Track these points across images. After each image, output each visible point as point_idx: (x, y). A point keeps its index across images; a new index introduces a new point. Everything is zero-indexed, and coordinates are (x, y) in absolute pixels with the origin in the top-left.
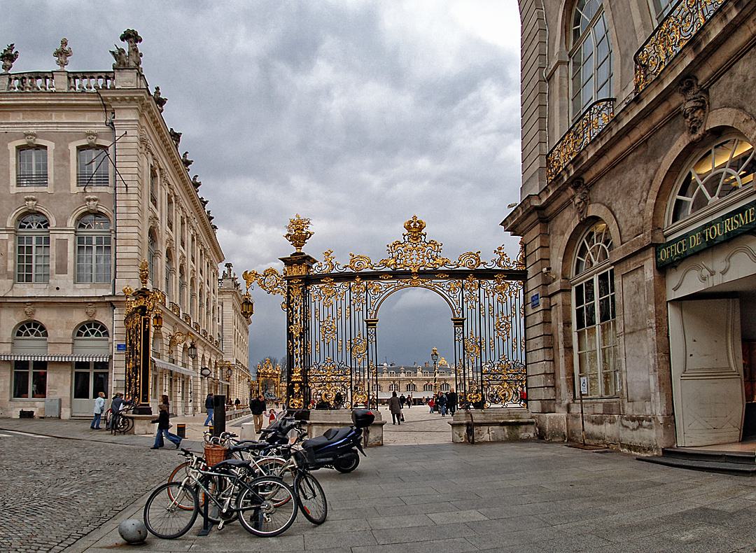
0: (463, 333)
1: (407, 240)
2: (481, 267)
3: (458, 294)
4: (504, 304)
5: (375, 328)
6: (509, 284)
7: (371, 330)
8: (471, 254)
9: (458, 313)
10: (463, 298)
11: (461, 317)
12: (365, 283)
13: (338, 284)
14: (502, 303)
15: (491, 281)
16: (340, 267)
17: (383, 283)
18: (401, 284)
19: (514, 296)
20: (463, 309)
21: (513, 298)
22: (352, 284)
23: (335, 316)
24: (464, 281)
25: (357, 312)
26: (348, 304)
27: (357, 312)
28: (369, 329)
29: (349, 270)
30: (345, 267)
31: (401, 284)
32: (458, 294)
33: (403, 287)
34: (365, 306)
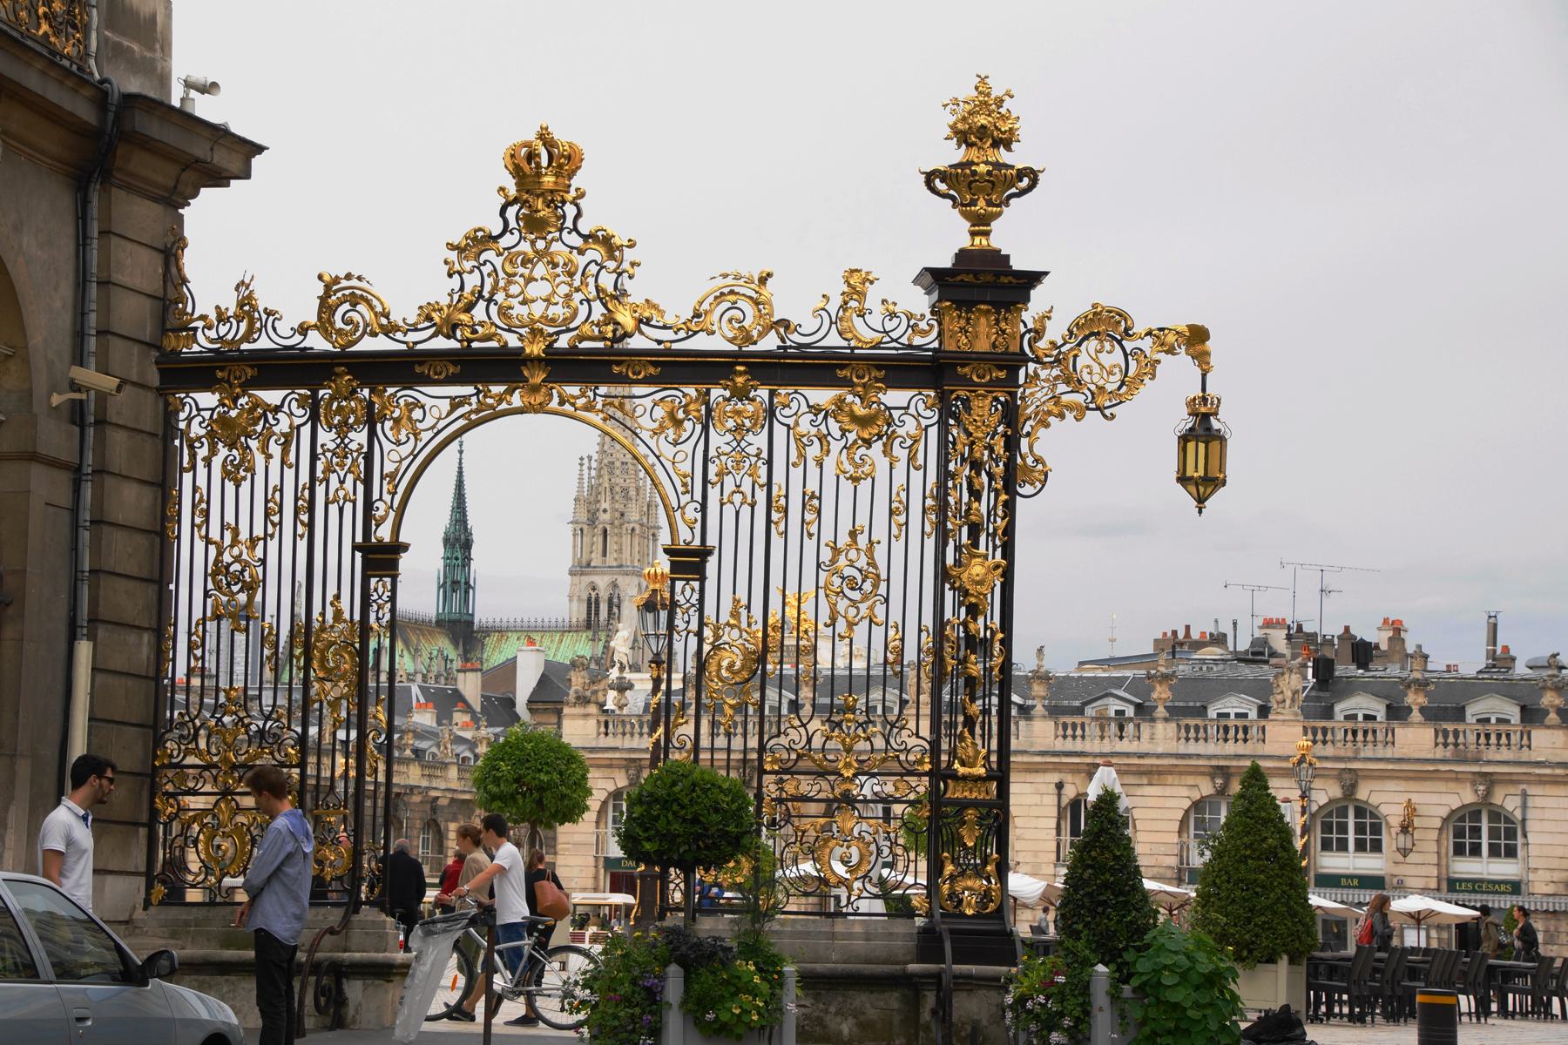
4: (865, 486)
7: (379, 586)
11: (697, 542)
14: (855, 480)
17: (435, 400)
21: (901, 467)
24: (717, 393)
30: (303, 330)
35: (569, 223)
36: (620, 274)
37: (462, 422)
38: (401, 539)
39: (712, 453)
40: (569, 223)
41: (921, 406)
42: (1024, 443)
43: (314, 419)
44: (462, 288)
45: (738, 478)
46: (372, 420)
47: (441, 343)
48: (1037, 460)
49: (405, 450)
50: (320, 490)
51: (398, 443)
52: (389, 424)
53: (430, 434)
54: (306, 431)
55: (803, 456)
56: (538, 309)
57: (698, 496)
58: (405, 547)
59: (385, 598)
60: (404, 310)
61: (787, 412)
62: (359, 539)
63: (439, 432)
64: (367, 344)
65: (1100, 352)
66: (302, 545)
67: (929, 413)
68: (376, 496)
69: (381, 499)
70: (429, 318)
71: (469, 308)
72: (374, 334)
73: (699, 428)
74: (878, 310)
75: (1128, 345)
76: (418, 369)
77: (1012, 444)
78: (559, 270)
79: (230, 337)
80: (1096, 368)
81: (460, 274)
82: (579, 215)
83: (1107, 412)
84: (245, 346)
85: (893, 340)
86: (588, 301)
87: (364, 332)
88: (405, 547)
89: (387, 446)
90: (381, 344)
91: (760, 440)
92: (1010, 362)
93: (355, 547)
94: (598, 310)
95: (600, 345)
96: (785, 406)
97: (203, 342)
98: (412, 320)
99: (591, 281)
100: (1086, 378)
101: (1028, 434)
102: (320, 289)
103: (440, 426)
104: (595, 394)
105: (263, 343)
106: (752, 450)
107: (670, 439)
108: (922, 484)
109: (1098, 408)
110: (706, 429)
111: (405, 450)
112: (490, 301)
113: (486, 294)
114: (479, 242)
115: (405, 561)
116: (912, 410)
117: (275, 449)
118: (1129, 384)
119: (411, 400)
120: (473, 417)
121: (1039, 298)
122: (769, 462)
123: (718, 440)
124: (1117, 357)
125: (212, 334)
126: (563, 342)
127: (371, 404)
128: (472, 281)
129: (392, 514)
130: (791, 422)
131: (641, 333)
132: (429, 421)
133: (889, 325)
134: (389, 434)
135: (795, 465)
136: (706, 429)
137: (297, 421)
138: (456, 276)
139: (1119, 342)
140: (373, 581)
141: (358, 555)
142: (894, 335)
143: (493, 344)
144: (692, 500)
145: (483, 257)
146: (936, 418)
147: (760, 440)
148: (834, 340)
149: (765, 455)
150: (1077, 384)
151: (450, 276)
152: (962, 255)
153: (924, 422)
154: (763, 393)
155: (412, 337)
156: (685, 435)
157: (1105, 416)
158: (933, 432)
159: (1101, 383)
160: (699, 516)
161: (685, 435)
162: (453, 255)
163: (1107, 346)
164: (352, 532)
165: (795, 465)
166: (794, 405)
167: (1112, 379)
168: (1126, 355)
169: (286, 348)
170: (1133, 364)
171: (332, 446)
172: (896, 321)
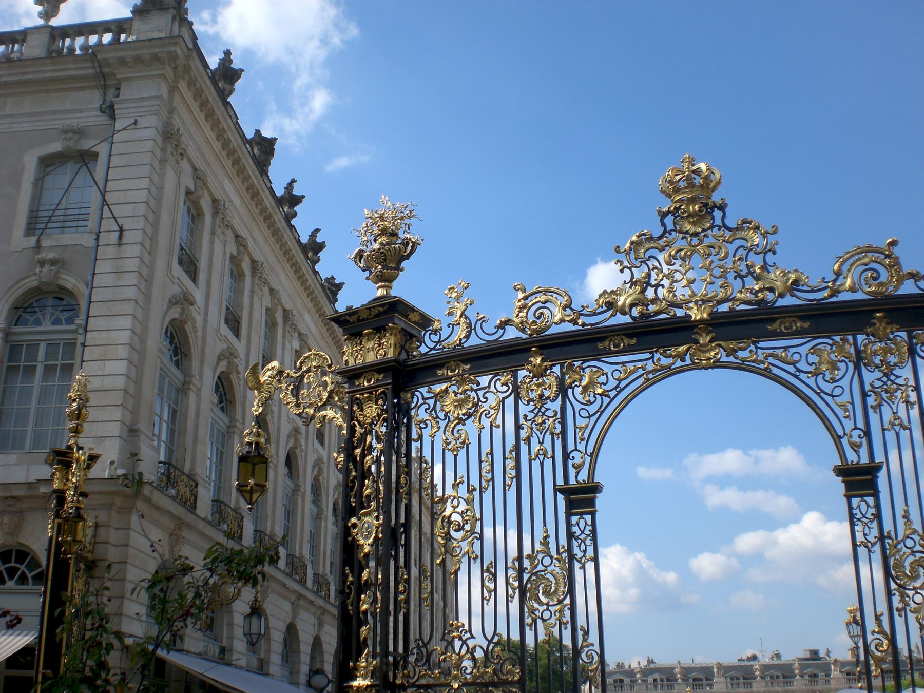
0: (878, 516)
1: (670, 226)
3: (845, 383)
5: (593, 514)
7: (581, 523)
9: (855, 447)
10: (864, 395)
12: (557, 369)
18: (665, 362)
20: (867, 433)
23: (475, 481)
24: (861, 338)
25: (536, 465)
26: (510, 441)
27: (536, 465)
28: (574, 519)
30: (504, 325)
31: (665, 362)
32: (845, 383)
33: (670, 372)
34: (558, 443)
46: (563, 390)
52: (578, 390)
54: (510, 402)
57: (861, 424)
59: (587, 532)
62: (560, 481)
68: (571, 447)
69: (576, 450)
73: (851, 365)
81: (630, 269)
89: (578, 407)
93: (557, 490)
103: (622, 385)
104: (757, 348)
106: (900, 381)
107: (827, 378)
113: (653, 282)
119: (594, 369)
129: (588, 459)
134: (580, 397)
144: (856, 428)
151: (622, 271)
160: (864, 441)
161: (841, 373)
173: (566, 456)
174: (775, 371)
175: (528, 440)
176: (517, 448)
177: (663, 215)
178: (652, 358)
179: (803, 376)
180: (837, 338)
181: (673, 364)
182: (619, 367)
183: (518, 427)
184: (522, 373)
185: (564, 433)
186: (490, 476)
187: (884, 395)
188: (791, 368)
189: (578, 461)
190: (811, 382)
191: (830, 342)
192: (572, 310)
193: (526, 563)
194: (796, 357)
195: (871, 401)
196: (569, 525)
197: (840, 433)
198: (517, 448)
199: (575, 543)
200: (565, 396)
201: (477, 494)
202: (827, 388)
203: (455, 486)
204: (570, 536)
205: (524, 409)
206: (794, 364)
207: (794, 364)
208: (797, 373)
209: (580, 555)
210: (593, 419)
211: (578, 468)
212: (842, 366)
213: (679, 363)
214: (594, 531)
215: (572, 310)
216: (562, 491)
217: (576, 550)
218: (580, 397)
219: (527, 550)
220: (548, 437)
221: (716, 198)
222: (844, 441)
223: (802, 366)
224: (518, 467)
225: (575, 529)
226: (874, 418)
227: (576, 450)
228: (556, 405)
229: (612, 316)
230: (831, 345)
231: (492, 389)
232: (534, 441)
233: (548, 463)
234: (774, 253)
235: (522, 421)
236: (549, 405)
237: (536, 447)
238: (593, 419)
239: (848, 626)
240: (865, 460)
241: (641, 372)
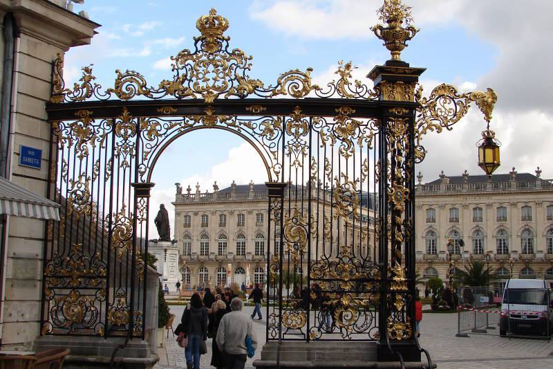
1: (199, 49)
2: (312, 94)
3: (276, 141)
4: (350, 159)
5: (148, 198)
6: (358, 125)
7: (142, 202)
8: (297, 72)
9: (277, 173)
10: (284, 147)
11: (280, 181)
12: (136, 120)
13: (98, 122)
14: (347, 156)
15: (330, 120)
16: (102, 91)
17: (163, 122)
18: (191, 122)
19: (365, 144)
22: (117, 120)
23: (90, 174)
25: (121, 169)
29: (114, 97)
30: (109, 92)
31: (191, 122)
32: (276, 141)
33: (191, 128)
34: (134, 160)
35: (224, 49)
36: (245, 69)
37: (176, 133)
38: (152, 181)
39: (286, 144)
40: (224, 49)
41: (373, 125)
42: (416, 140)
43: (114, 131)
44: (178, 74)
45: (297, 155)
46: (137, 132)
47: (169, 97)
48: (422, 148)
49: (153, 143)
50: (116, 160)
51: (151, 140)
52: (146, 133)
53: (163, 137)
54: (110, 136)
55: (325, 144)
56: (211, 83)
58: (153, 185)
60: (153, 83)
61: (317, 126)
62: (133, 181)
63: (168, 136)
64: (136, 98)
65: (445, 103)
66: (108, 182)
67: (376, 128)
68: (140, 162)
69: (142, 164)
70: (163, 87)
71: (183, 82)
72: (139, 94)
73: (280, 132)
74: (354, 84)
75: (456, 100)
76: (159, 110)
77: (411, 138)
78: (219, 68)
79: (80, 95)
80: (443, 110)
81: (177, 70)
82: (227, 46)
83: (449, 127)
84: (87, 100)
85: (361, 96)
86: (232, 80)
87: (135, 93)
88: (153, 185)
90: (143, 98)
91: (306, 139)
92: (412, 107)
94: (236, 83)
95: (237, 97)
96: (317, 123)
97: (68, 99)
98: (156, 88)
99: (233, 72)
100: (439, 113)
101: (417, 137)
102: (116, 76)
103: (168, 133)
105: (93, 98)
106: (303, 142)
108: (373, 159)
109: (445, 126)
110: (283, 133)
111: (153, 143)
112: (190, 80)
113: (188, 78)
114: (184, 55)
115: (152, 191)
116: (369, 126)
117: (97, 144)
118: (457, 116)
120: (183, 130)
121: (422, 80)
122: (310, 148)
123: (288, 138)
124: (452, 105)
125: (72, 95)
126: (222, 97)
127: (138, 126)
128: (182, 72)
129: (148, 170)
130: (319, 130)
131: (255, 93)
132: (163, 131)
133: (359, 90)
134: (146, 137)
135: (321, 147)
136: (283, 133)
137: (107, 132)
138: (175, 71)
139: (453, 99)
140: (139, 199)
141: (132, 188)
142: (361, 94)
143: (191, 97)
145: (186, 63)
146: (378, 131)
147: (306, 139)
148: (336, 96)
149: (308, 144)
150: (436, 117)
151: (173, 70)
152: (388, 63)
153: (374, 132)
154: (308, 119)
155: (155, 95)
156: (275, 136)
157: (448, 128)
158: (377, 136)
159: (446, 115)
160: (281, 170)
161: (275, 136)
162: (174, 62)
163: (448, 101)
164: (129, 175)
165: (321, 147)
166: (321, 122)
167: (450, 114)
168: (455, 104)
169: (102, 100)
170: (458, 107)
171: (120, 144)
172: (361, 89)
173: (137, 167)
174: (243, 132)
175: (119, 155)
176: (112, 160)
177: (197, 41)
178: (184, 120)
179: (256, 136)
180: (275, 118)
181: (194, 124)
182: (167, 122)
183: (114, 149)
184: (117, 120)
185: (137, 155)
186: (97, 173)
187: (294, 148)
188: (251, 131)
189: (143, 170)
190: (260, 139)
191: (271, 119)
192: (146, 88)
193: (113, 219)
194: (254, 126)
195: (286, 151)
196: (136, 202)
197: (270, 166)
198: (112, 160)
199: (138, 211)
200: (139, 136)
201: (90, 182)
202: (268, 143)
203: (80, 177)
204: (136, 207)
205: (118, 140)
206: (253, 129)
207: (253, 129)
208: (253, 134)
209: (140, 217)
210: (153, 149)
211: (142, 174)
212: (276, 132)
213: (197, 124)
214: (148, 206)
215: (146, 88)
216: (133, 185)
217: (138, 214)
218: (146, 137)
219: (114, 211)
220: (129, 156)
221: (225, 35)
222: (272, 170)
223: (257, 130)
224: (112, 169)
225: (139, 204)
226: (287, 159)
227: (142, 164)
228: (133, 140)
229: (165, 95)
230: (272, 121)
231: (102, 126)
232: (121, 157)
233: (128, 169)
234: (249, 70)
235: (116, 146)
236: (130, 139)
237: (122, 159)
238: (153, 149)
239: (189, 224)
240: (280, 181)
241: (178, 126)
